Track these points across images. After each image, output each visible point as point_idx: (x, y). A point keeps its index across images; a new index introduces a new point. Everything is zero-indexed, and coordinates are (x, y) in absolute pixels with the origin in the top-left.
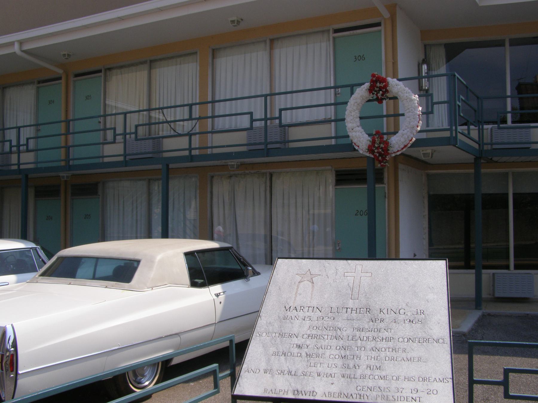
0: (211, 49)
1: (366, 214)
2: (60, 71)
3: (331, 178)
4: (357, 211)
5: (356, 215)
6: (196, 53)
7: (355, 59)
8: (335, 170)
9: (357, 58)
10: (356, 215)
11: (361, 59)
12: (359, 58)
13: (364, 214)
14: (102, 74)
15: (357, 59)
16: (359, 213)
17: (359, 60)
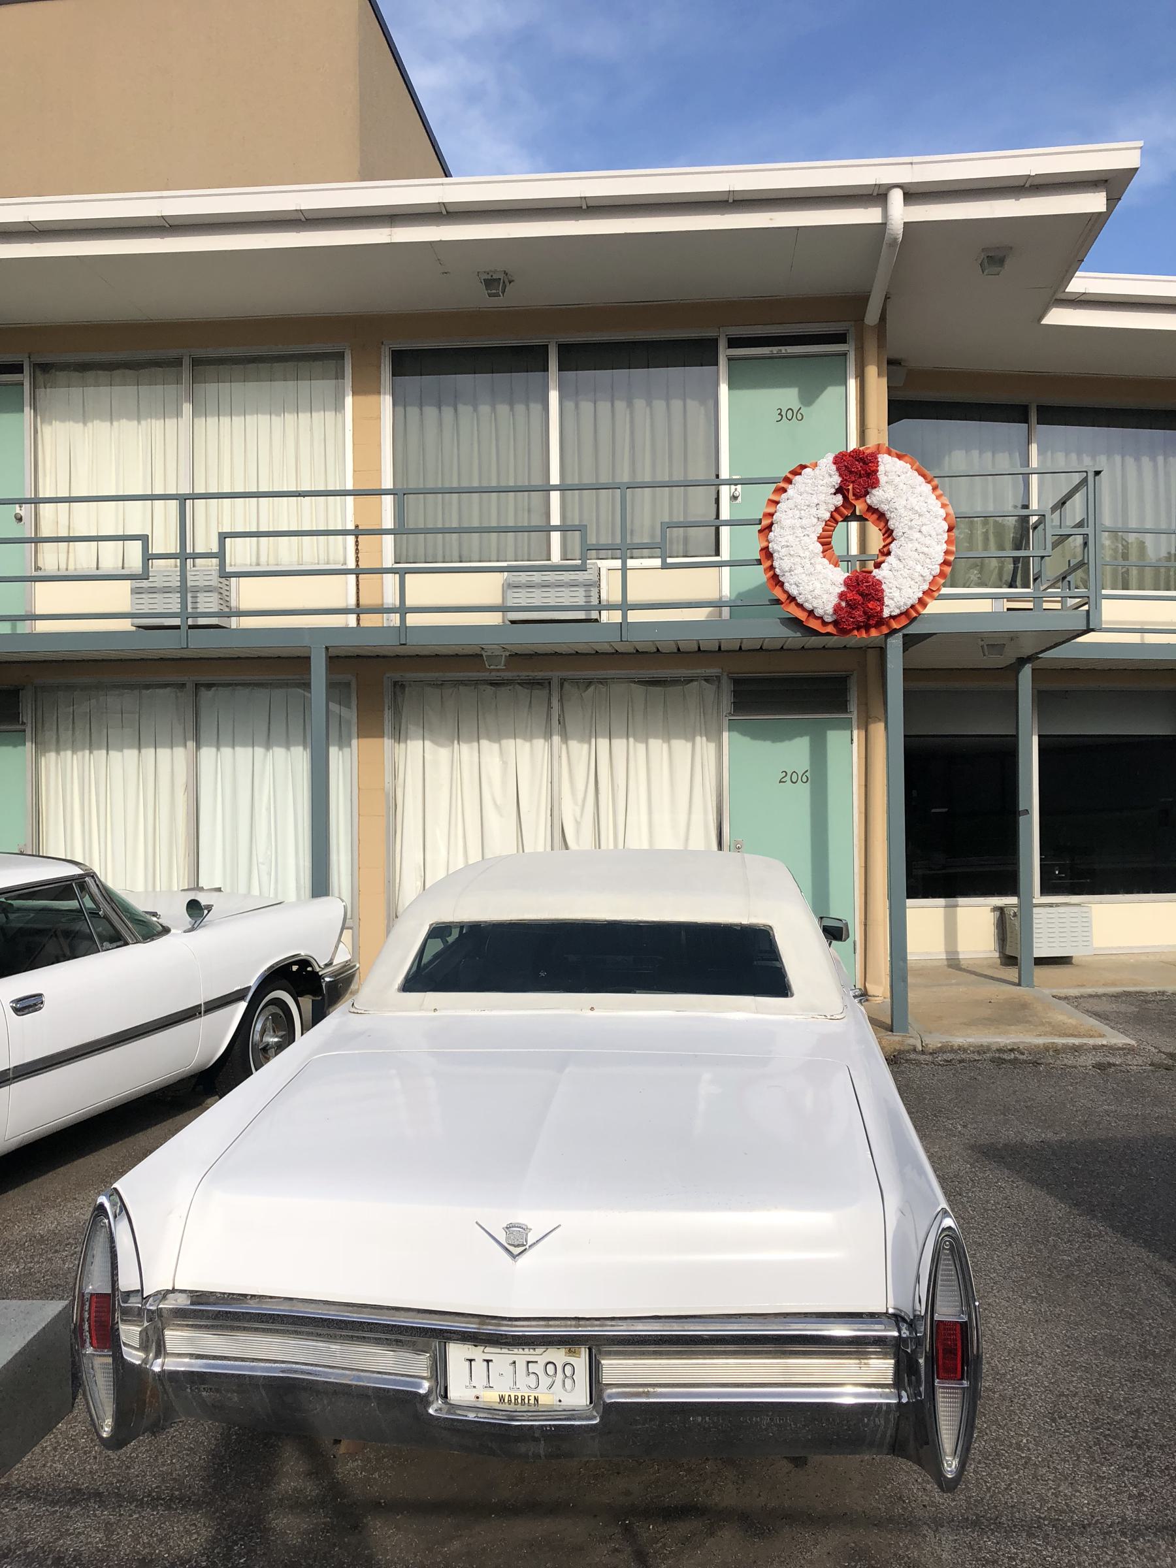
0: (387, 350)
1: (804, 779)
4: (784, 774)
5: (780, 782)
6: (340, 356)
7: (780, 417)
8: (730, 678)
9: (784, 413)
10: (780, 782)
12: (790, 414)
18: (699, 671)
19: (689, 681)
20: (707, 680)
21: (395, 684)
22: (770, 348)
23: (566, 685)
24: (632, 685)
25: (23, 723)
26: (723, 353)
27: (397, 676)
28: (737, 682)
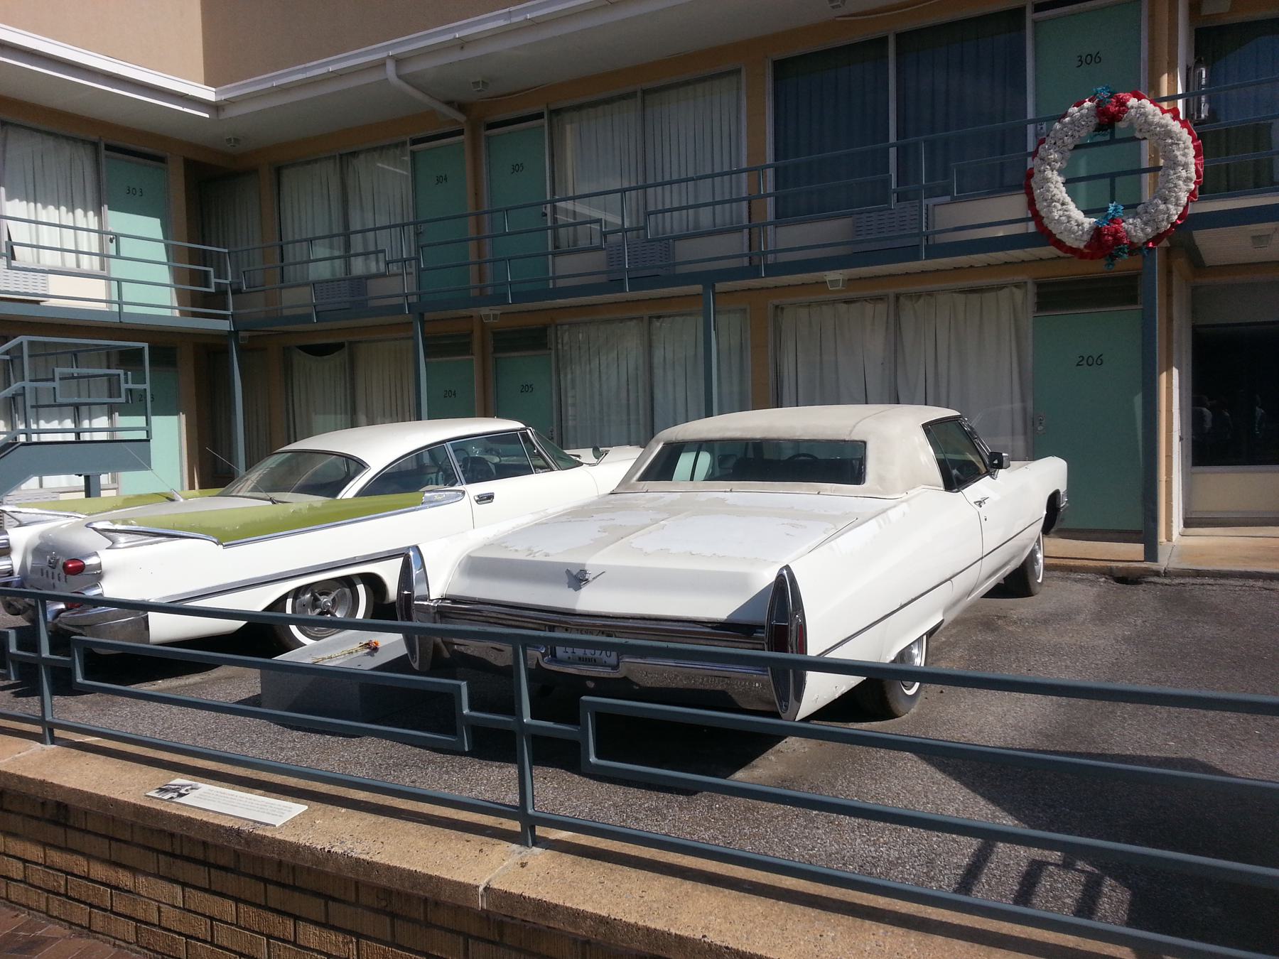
2: (461, 118)
3: (1025, 299)
6: (738, 71)
10: (1078, 365)
11: (1093, 62)
13: (1093, 360)
14: (545, 121)
15: (1084, 62)
16: (1084, 362)
17: (1089, 64)
18: (1008, 279)
19: (1001, 287)
20: (1017, 286)
21: (777, 307)
22: (1071, 7)
23: (902, 299)
24: (955, 295)
25: (550, 349)
26: (1030, 16)
27: (776, 302)
28: (1039, 285)
